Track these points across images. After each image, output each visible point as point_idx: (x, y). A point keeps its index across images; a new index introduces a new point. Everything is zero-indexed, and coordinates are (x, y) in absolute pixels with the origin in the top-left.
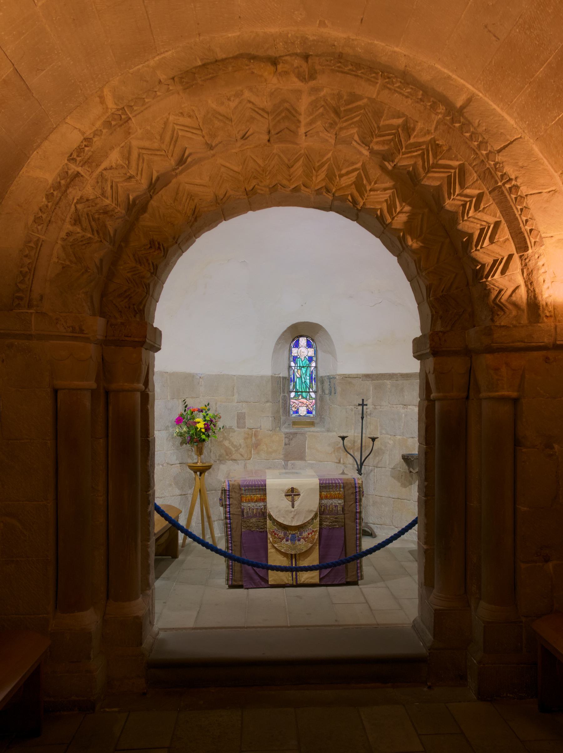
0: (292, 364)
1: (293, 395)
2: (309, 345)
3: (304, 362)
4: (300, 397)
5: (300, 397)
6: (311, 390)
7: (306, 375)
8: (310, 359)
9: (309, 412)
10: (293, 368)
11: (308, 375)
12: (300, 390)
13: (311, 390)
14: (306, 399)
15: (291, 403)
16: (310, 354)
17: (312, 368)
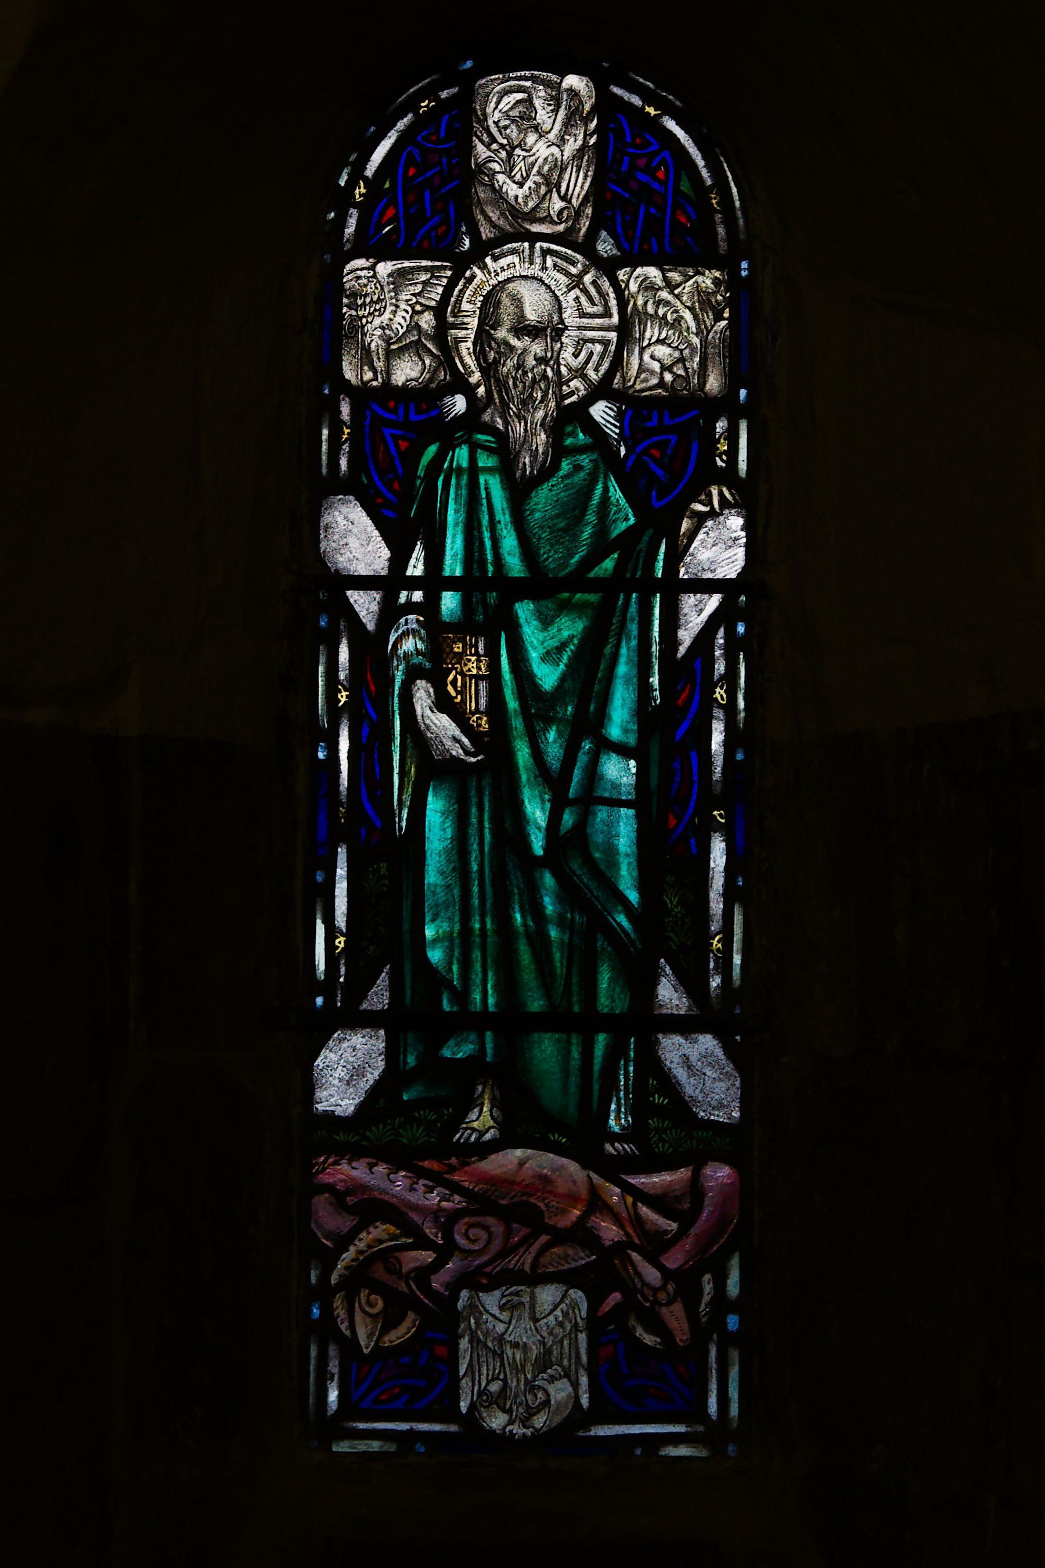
0: (355, 540)
1: (345, 1071)
2: (634, 213)
3: (543, 500)
4: (482, 1120)
5: (482, 1120)
6: (669, 995)
7: (588, 725)
8: (663, 450)
9: (625, 1374)
10: (365, 605)
11: (619, 721)
12: (485, 995)
13: (669, 995)
14: (584, 1140)
15: (327, 1218)
16: (654, 360)
17: (697, 612)
